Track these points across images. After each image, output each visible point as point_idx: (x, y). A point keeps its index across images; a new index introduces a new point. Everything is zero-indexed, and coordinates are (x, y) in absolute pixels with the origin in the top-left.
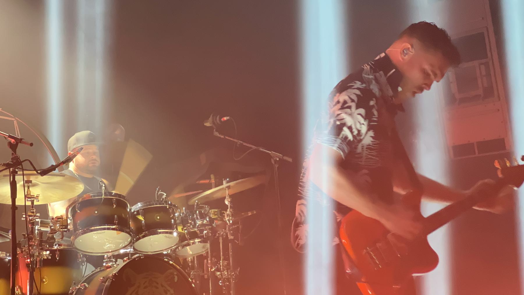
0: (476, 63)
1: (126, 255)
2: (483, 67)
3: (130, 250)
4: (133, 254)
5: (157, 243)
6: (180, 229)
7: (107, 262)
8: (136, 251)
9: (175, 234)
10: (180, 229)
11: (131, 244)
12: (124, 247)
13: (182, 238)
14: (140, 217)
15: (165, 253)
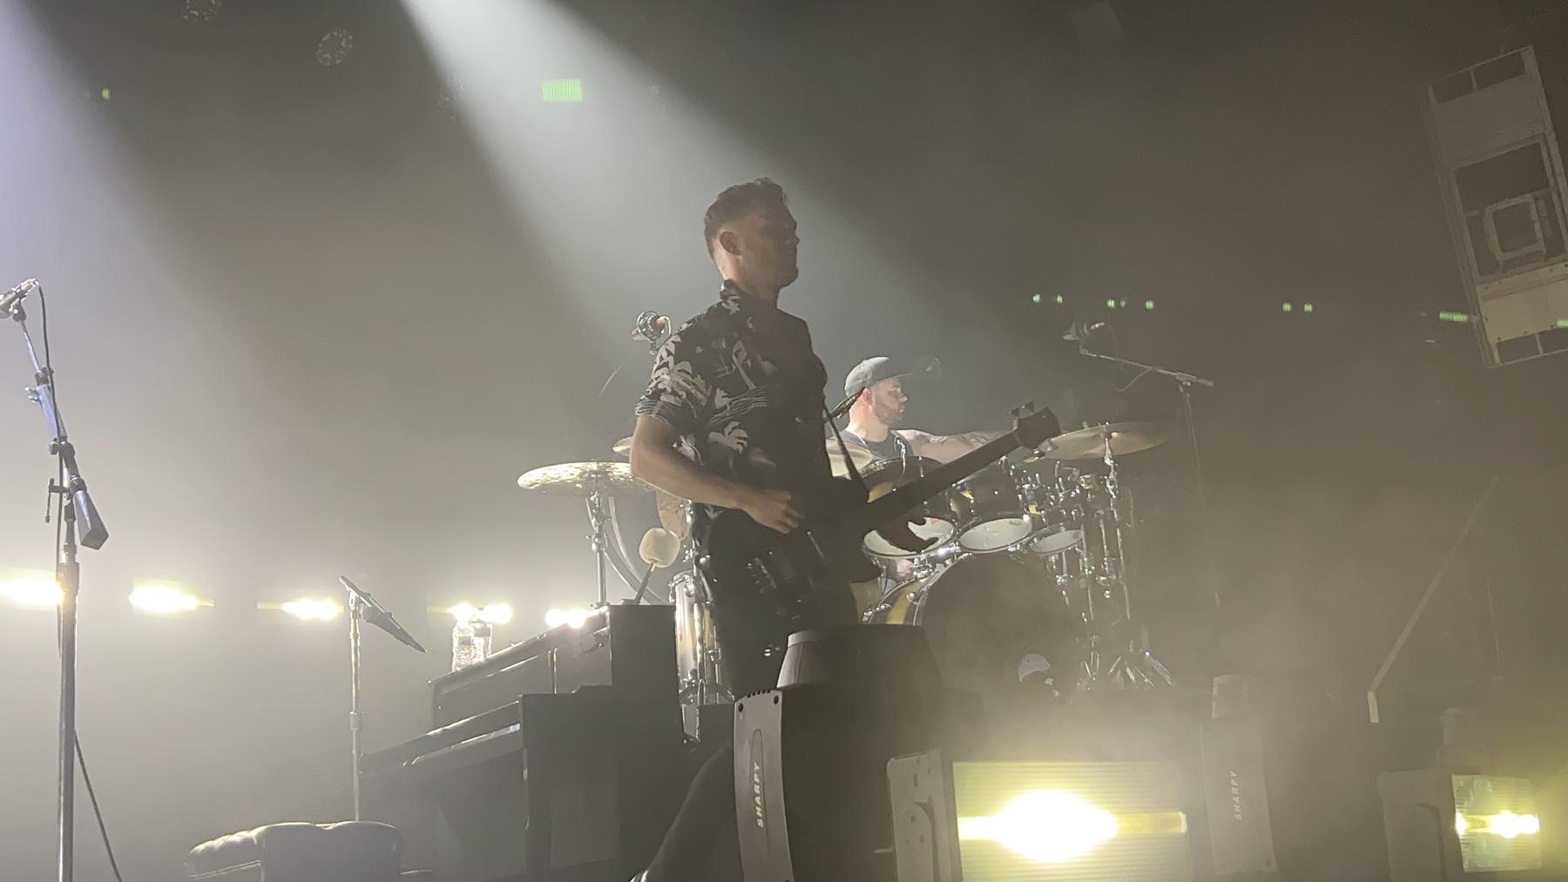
0: (1528, 197)
1: (950, 556)
2: (1541, 202)
3: (954, 548)
4: (959, 555)
5: (997, 534)
6: (1033, 509)
7: (919, 569)
8: (964, 549)
9: (1026, 518)
10: (1033, 509)
11: (955, 538)
12: (945, 544)
13: (1037, 523)
14: (967, 495)
15: (1011, 549)
